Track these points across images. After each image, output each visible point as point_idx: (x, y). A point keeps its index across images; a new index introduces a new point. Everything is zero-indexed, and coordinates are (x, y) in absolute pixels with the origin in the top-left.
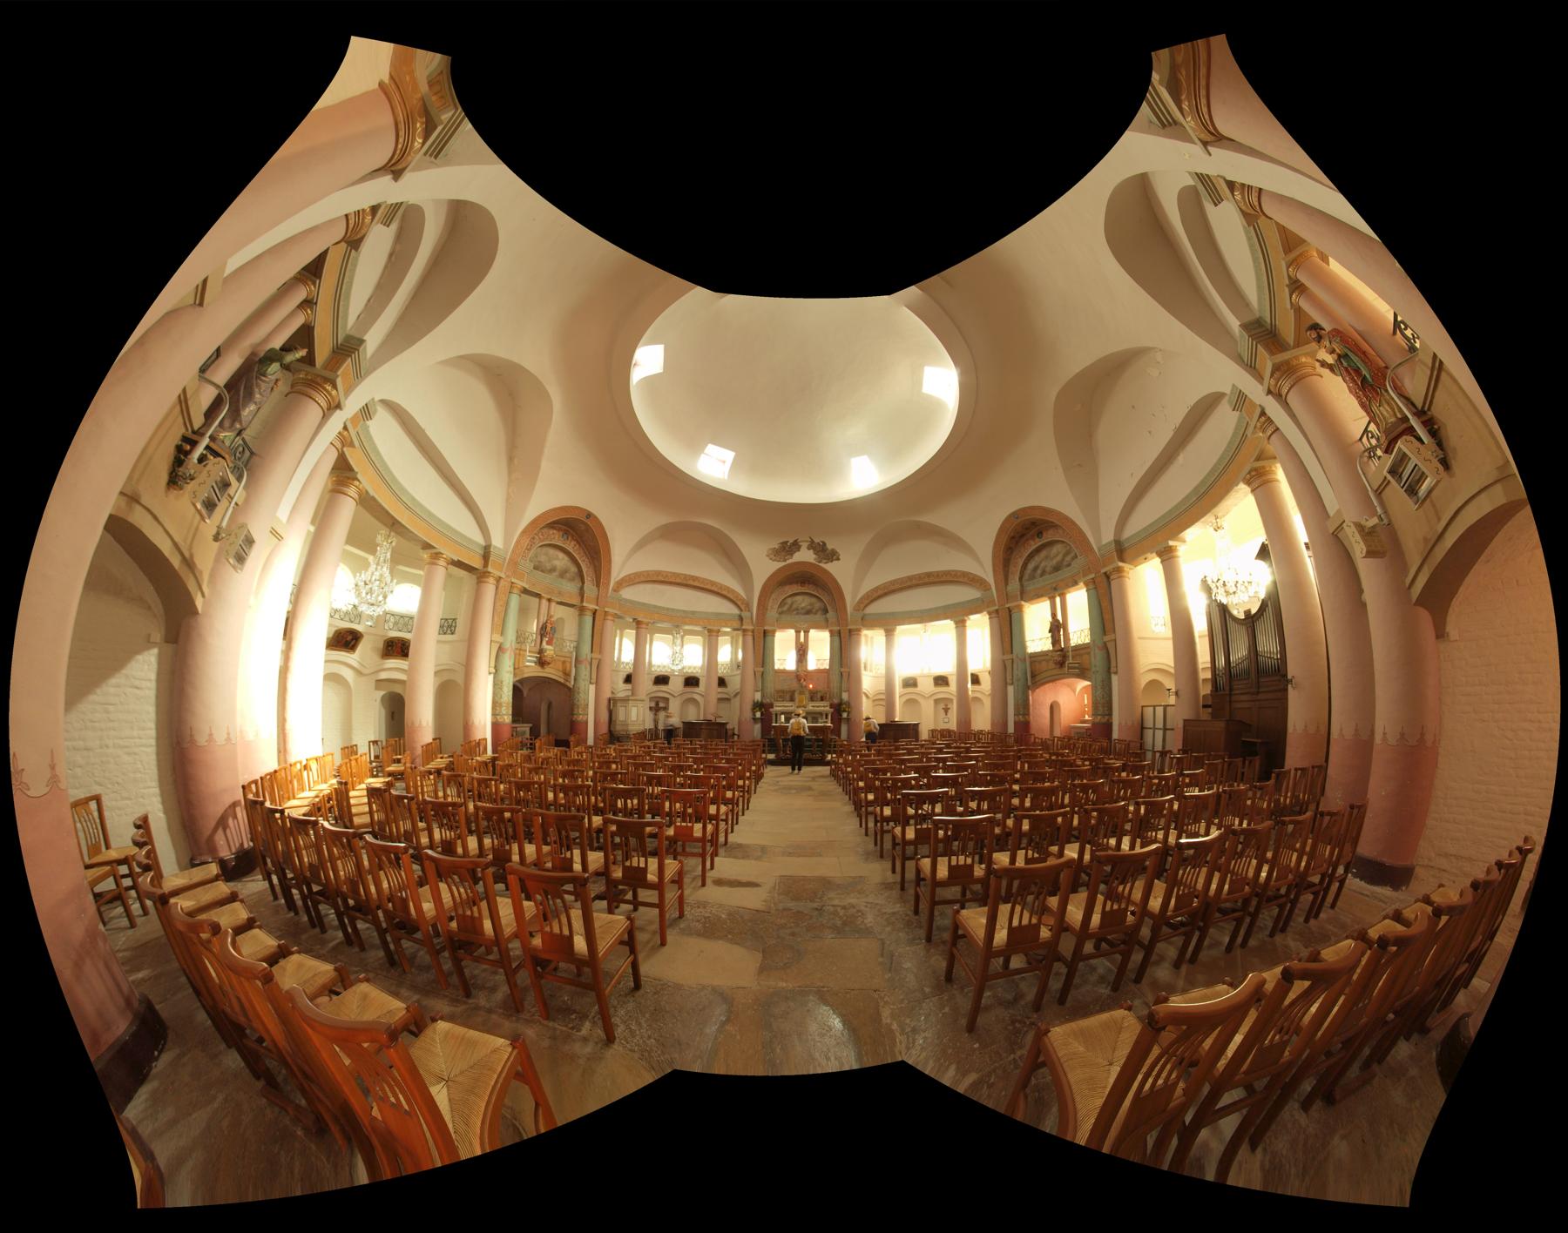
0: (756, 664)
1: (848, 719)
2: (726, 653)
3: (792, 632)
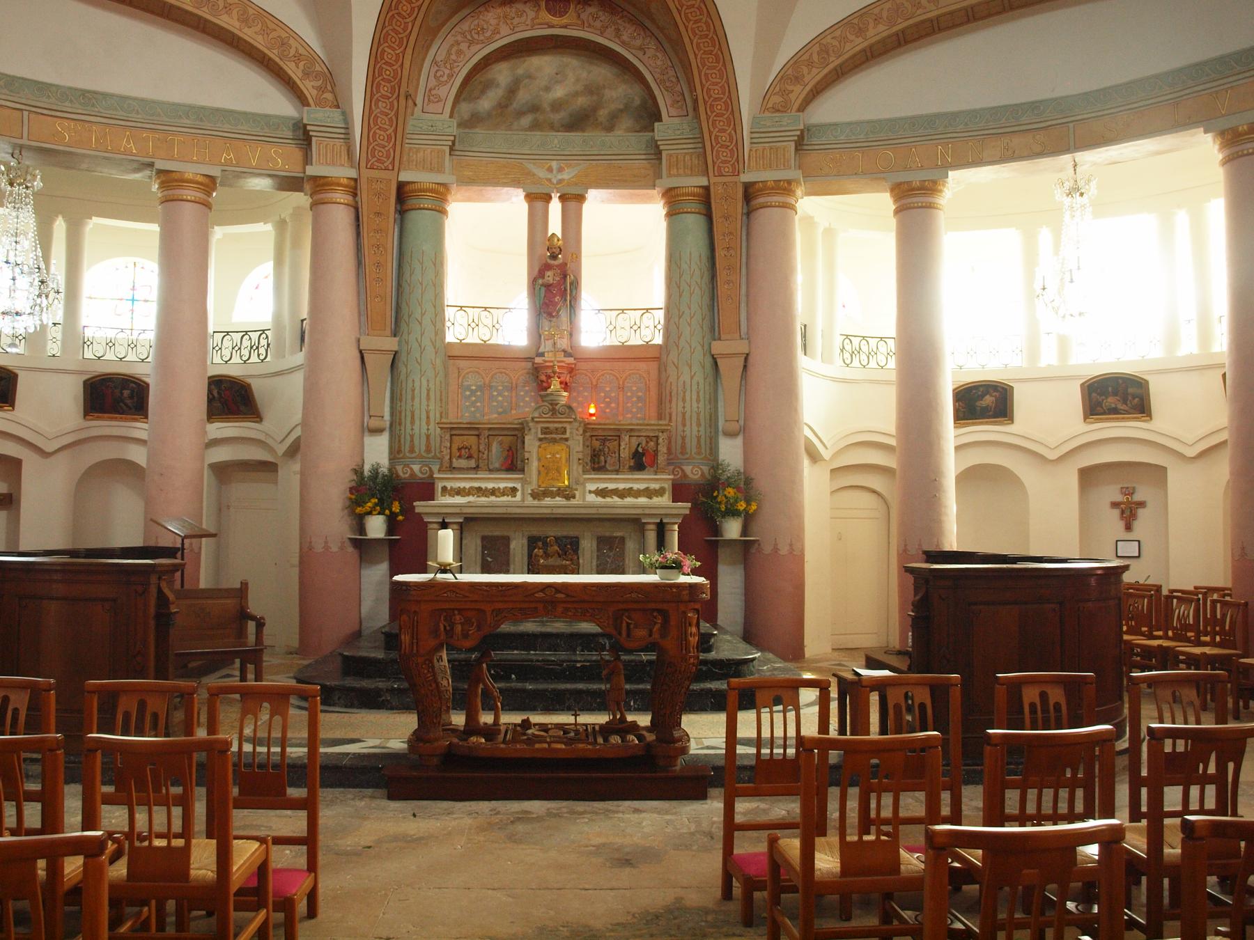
1: (746, 549)
2: (252, 290)
3: (511, 207)
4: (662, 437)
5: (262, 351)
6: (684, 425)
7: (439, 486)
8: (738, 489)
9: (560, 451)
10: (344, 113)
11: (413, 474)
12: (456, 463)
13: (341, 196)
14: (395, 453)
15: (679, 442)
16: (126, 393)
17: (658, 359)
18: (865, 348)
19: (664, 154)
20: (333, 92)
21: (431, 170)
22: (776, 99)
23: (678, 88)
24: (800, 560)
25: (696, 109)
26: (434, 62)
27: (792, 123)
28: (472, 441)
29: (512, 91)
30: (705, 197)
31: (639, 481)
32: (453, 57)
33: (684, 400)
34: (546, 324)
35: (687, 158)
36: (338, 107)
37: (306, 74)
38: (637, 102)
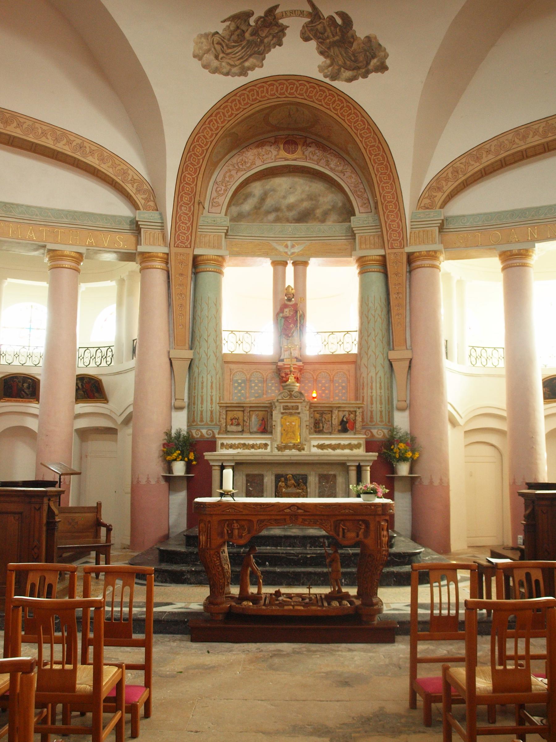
0: (174, 338)
1: (412, 482)
4: (359, 412)
5: (109, 359)
6: (372, 404)
7: (219, 442)
8: (407, 444)
9: (294, 421)
10: (161, 214)
11: (202, 436)
12: (230, 428)
13: (158, 264)
14: (191, 422)
15: (369, 414)
16: (25, 385)
17: (354, 362)
18: (484, 354)
19: (357, 235)
20: (154, 201)
21: (214, 247)
22: (427, 201)
23: (365, 196)
24: (446, 488)
25: (376, 208)
26: (216, 182)
27: (437, 215)
28: (239, 414)
29: (263, 199)
30: (383, 262)
31: (345, 439)
32: (227, 179)
33: (372, 389)
34: (285, 342)
35: (372, 238)
36: (157, 210)
37: (138, 191)
38: (340, 204)
